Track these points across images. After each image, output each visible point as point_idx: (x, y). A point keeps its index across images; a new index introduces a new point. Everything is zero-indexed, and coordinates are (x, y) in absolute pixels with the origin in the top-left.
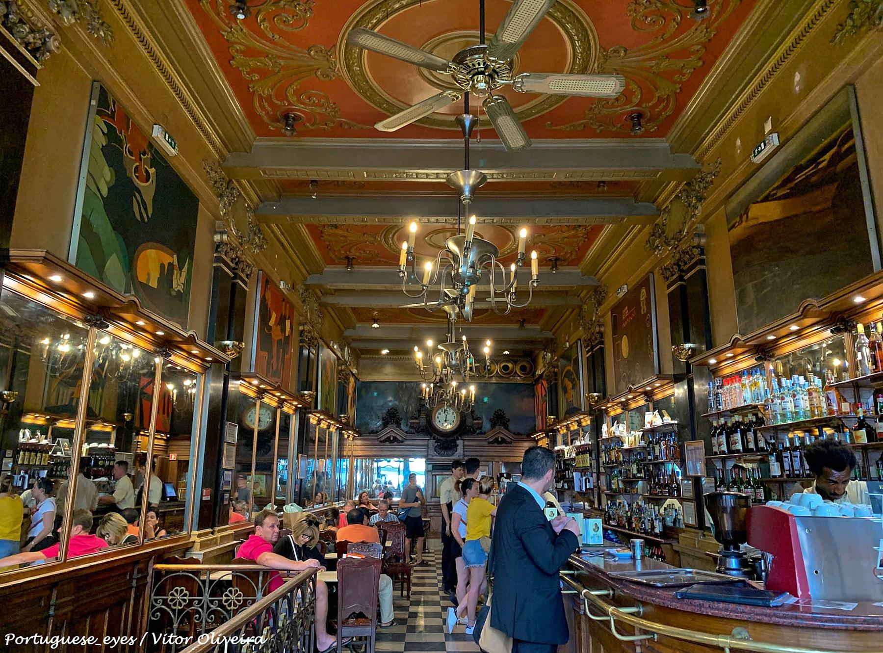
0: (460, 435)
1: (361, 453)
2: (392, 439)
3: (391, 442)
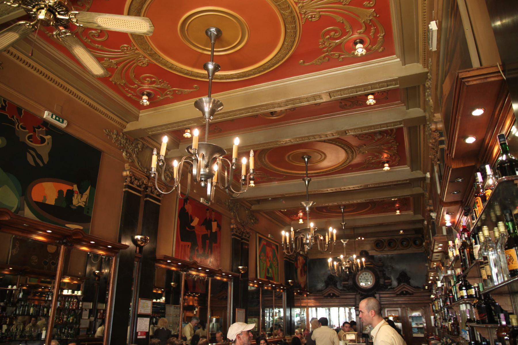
0: (378, 291)
1: (313, 305)
2: (332, 295)
3: (332, 297)
